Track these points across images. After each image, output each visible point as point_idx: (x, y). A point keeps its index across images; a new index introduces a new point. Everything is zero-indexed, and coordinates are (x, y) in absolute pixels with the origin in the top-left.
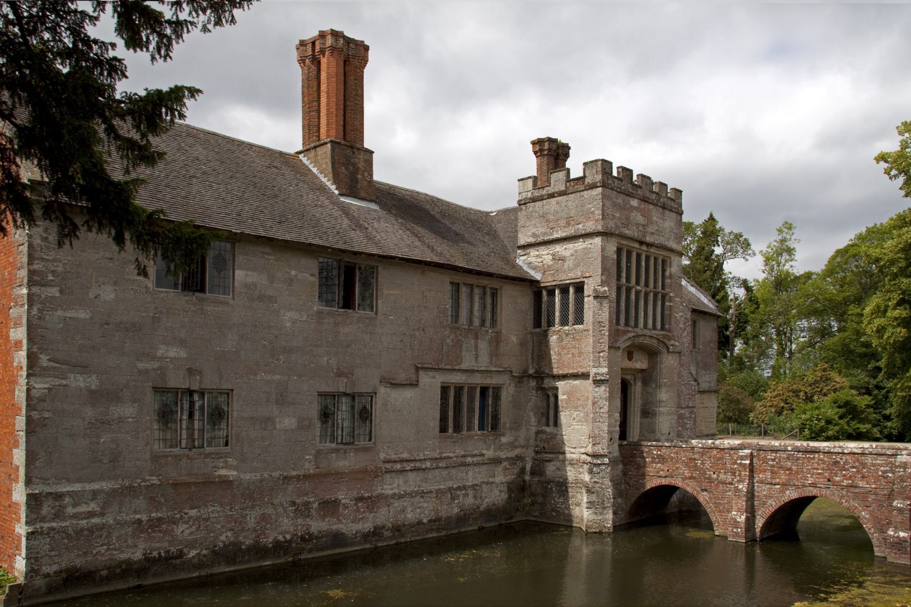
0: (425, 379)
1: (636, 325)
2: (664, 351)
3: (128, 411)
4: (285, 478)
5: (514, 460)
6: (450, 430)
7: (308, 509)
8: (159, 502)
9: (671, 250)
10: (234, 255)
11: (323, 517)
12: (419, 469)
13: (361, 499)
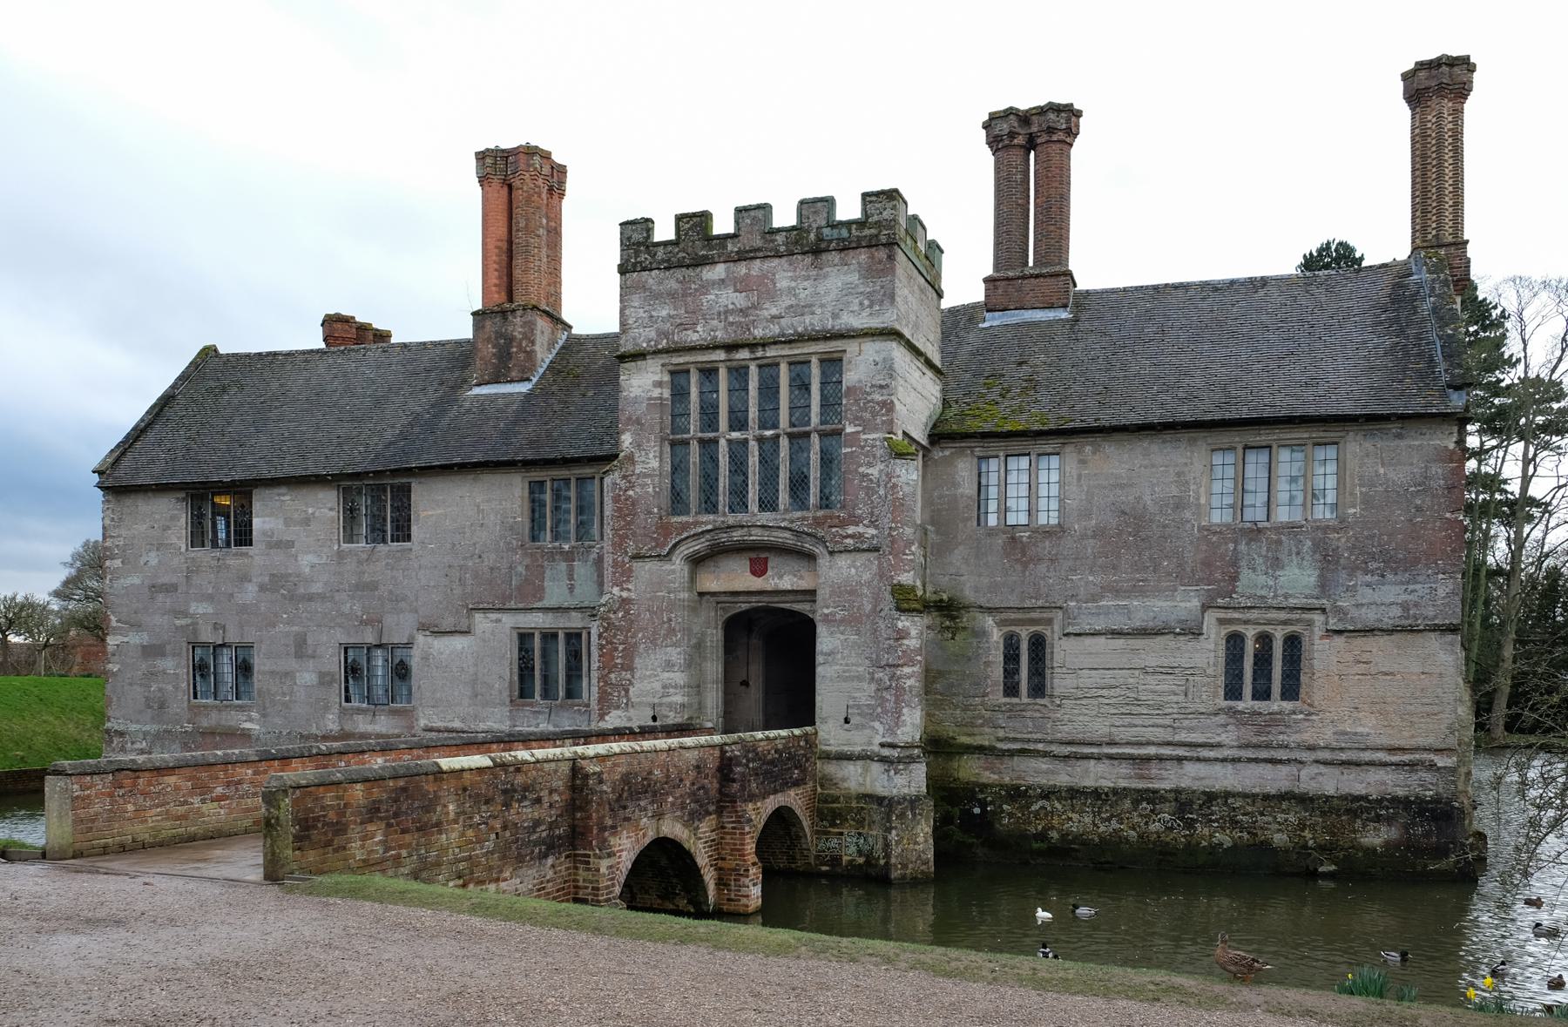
0: (481, 622)
3: (168, 664)
6: (537, 696)
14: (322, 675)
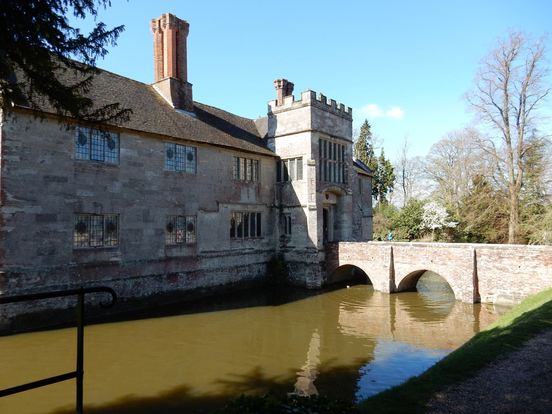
1: (330, 181)
2: (345, 194)
3: (60, 227)
4: (148, 261)
5: (269, 252)
6: (236, 236)
7: (161, 279)
8: (77, 276)
9: (348, 141)
10: (119, 140)
11: (170, 282)
12: (220, 256)
13: (188, 273)
14: (157, 230)
